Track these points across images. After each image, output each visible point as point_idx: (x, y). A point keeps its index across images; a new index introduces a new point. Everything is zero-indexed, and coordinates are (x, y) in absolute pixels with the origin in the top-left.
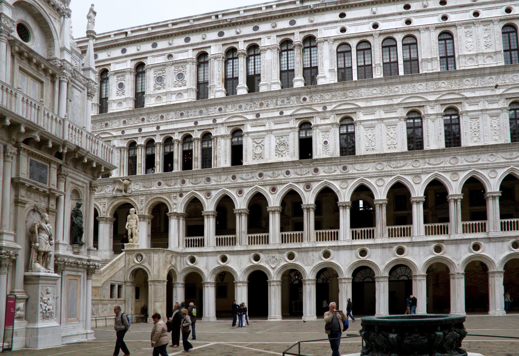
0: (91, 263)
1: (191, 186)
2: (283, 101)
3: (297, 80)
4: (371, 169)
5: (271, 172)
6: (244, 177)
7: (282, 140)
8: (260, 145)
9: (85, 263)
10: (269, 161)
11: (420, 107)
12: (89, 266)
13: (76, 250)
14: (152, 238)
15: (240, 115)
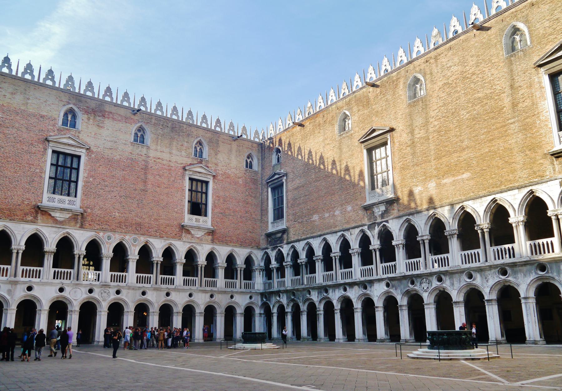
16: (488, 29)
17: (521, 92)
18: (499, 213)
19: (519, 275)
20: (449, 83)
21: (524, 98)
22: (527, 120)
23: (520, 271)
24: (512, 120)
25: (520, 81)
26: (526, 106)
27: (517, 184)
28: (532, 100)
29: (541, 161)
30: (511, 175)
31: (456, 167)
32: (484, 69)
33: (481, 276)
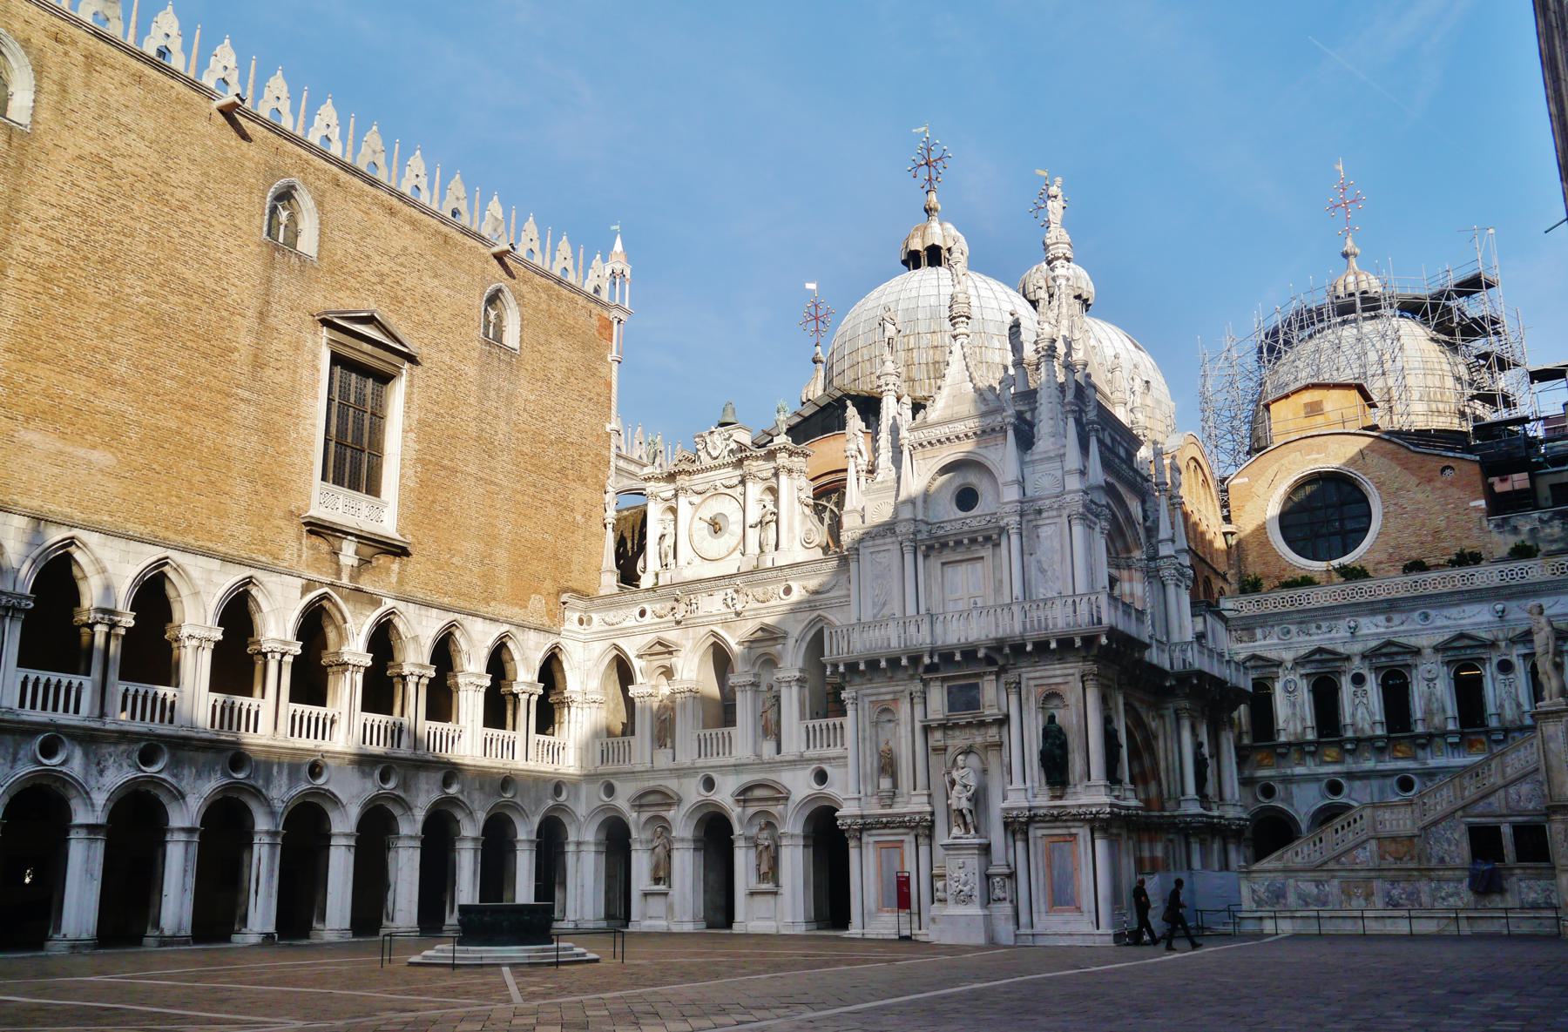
9: (1074, 811)
16: (245, 136)
17: (276, 345)
18: (153, 595)
19: (186, 772)
20: (109, 167)
21: (279, 365)
22: (275, 417)
23: (192, 762)
24: (247, 394)
25: (280, 317)
26: (280, 385)
27: (222, 549)
28: (294, 381)
29: (282, 523)
30: (214, 520)
31: (77, 416)
32: (214, 223)
33: (86, 755)
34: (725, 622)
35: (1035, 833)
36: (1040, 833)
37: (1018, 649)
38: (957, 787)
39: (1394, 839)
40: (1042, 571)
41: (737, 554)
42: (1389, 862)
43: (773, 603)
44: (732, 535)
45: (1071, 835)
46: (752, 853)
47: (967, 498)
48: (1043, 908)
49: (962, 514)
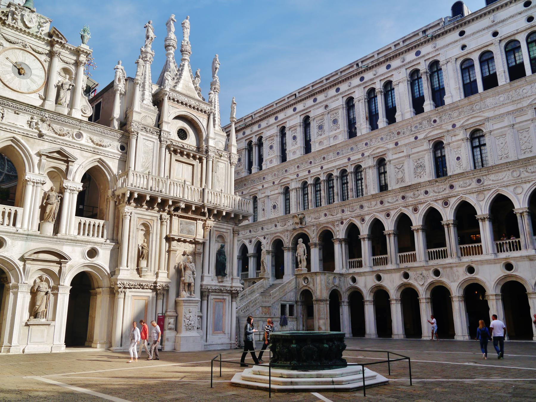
0: (233, 289)
1: (350, 215)
2: (416, 127)
3: (427, 105)
4: (506, 177)
5: (412, 193)
6: (390, 201)
7: (419, 162)
8: (401, 169)
9: (229, 289)
10: (410, 184)
11: (480, 125)
12: (232, 291)
13: (220, 280)
14: (324, 262)
15: (382, 146)
34: (26, 136)
35: (211, 297)
36: (213, 297)
37: (220, 212)
38: (188, 272)
39: (265, 307)
40: (219, 181)
41: (35, 96)
42: (263, 315)
43: (65, 138)
44: (33, 81)
45: (224, 299)
46: (28, 297)
47: (182, 134)
48: (211, 332)
49: (179, 140)
